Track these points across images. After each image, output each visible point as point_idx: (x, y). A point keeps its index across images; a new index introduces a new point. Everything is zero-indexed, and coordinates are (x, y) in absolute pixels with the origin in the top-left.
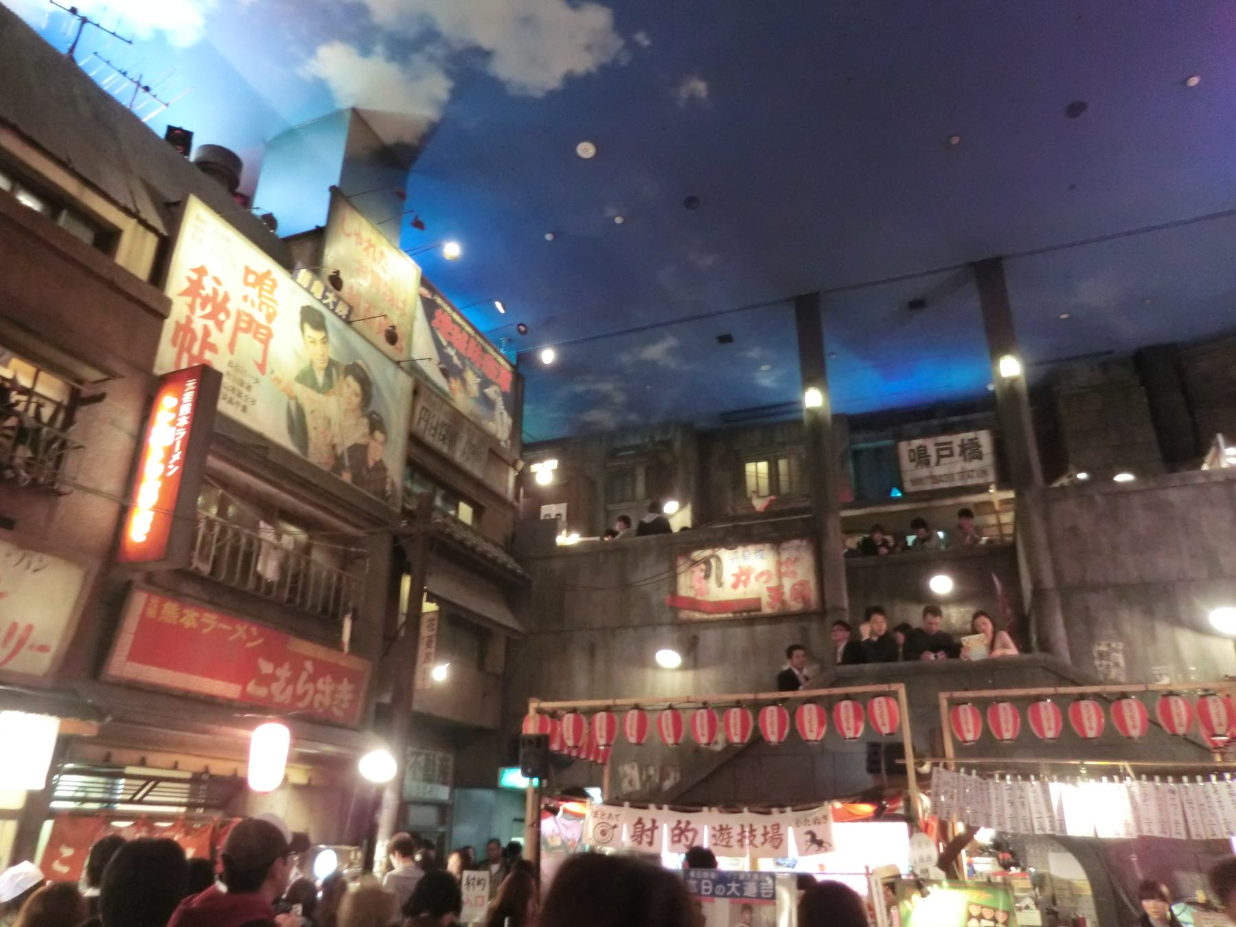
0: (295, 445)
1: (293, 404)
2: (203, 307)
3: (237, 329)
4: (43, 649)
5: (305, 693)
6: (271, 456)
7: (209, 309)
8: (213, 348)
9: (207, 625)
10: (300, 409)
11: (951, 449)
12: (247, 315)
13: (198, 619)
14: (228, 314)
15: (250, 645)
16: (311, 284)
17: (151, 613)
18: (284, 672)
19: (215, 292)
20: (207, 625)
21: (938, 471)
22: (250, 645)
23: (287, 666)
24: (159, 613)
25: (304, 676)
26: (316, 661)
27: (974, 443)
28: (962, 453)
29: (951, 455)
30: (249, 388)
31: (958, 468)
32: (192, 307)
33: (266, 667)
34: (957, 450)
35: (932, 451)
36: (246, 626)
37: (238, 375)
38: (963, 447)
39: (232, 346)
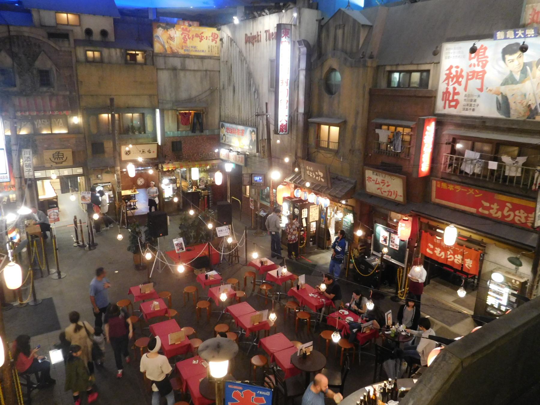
0: (501, 115)
1: (500, 98)
2: (452, 81)
3: (468, 80)
4: (401, 196)
5: (509, 215)
6: (487, 124)
7: (455, 80)
8: (458, 94)
9: (457, 189)
10: (505, 99)
12: (471, 72)
13: (454, 188)
14: (462, 77)
15: (476, 196)
16: (506, 34)
17: (439, 186)
18: (495, 206)
19: (457, 72)
20: (457, 189)
22: (476, 196)
23: (496, 204)
24: (441, 186)
25: (506, 209)
26: (512, 204)
30: (475, 101)
32: (448, 84)
33: (487, 204)
36: (473, 190)
37: (470, 98)
39: (465, 89)
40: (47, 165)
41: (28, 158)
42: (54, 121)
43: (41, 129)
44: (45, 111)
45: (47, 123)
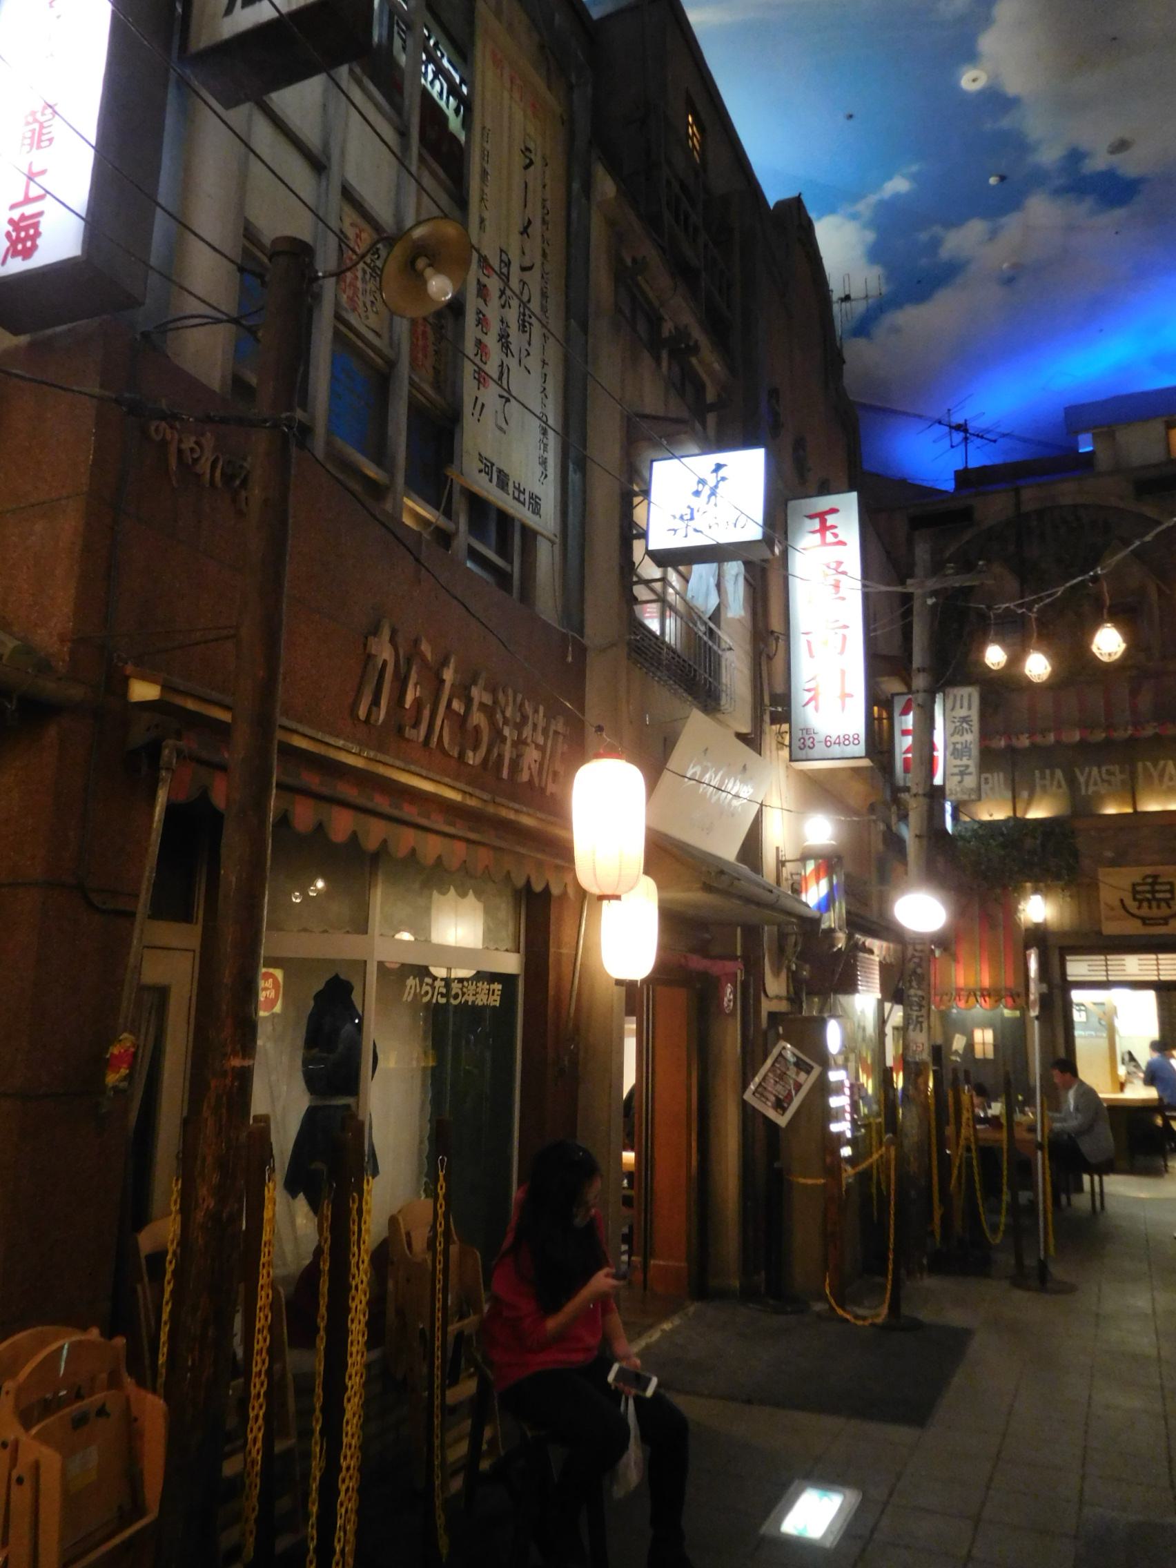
40: (1111, 928)
41: (965, 719)
42: (1145, 768)
43: (1100, 799)
44: (1110, 727)
45: (1120, 777)
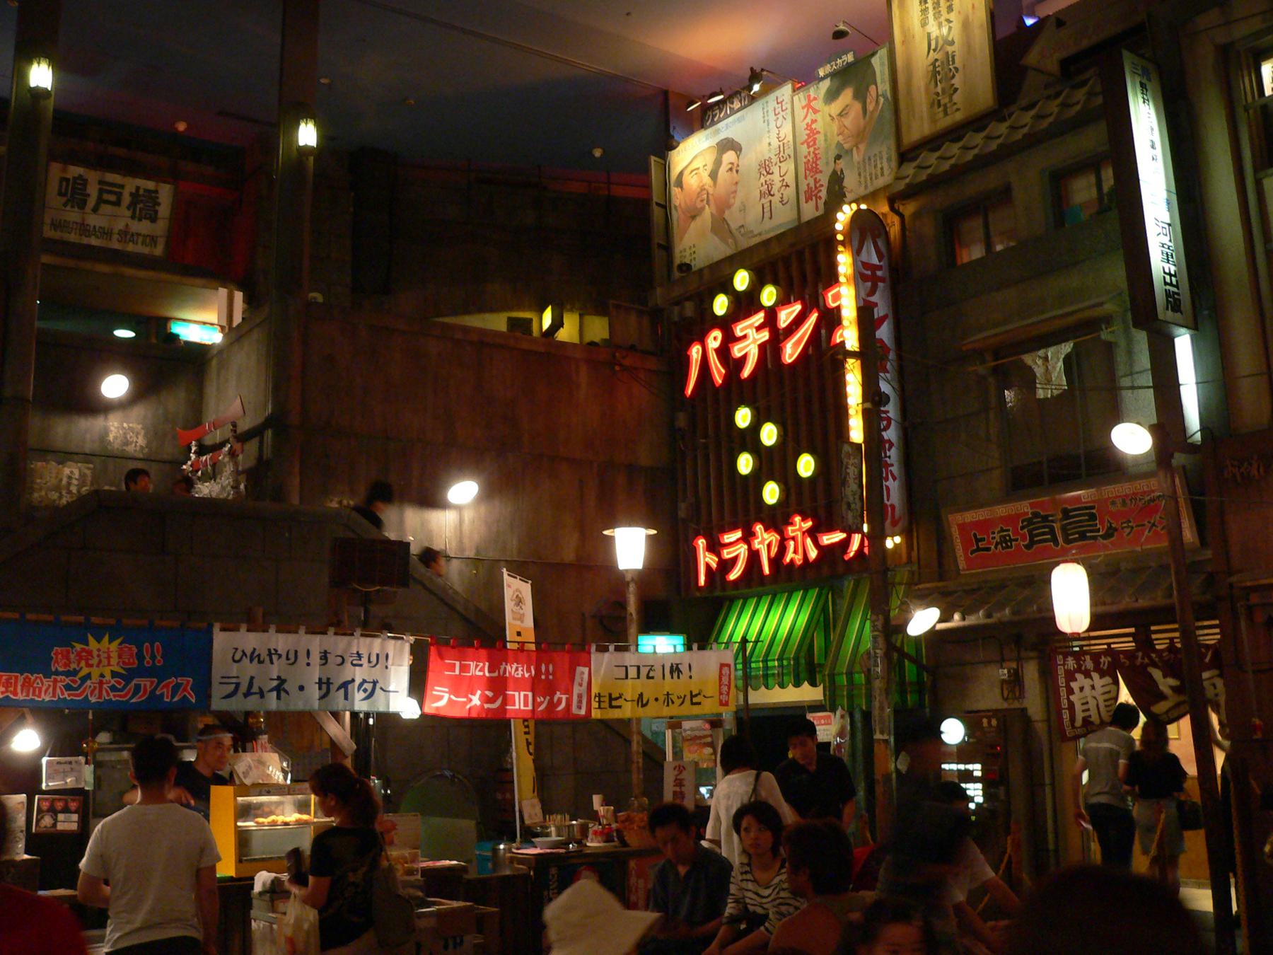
11: (119, 195)
21: (94, 221)
27: (152, 196)
28: (132, 205)
29: (117, 203)
31: (120, 225)
34: (127, 199)
35: (93, 191)
38: (135, 195)
